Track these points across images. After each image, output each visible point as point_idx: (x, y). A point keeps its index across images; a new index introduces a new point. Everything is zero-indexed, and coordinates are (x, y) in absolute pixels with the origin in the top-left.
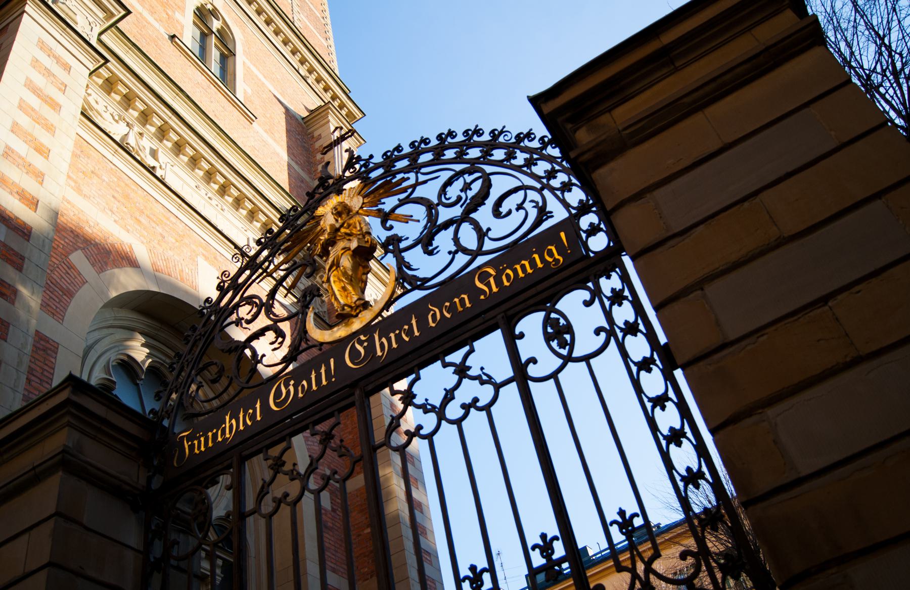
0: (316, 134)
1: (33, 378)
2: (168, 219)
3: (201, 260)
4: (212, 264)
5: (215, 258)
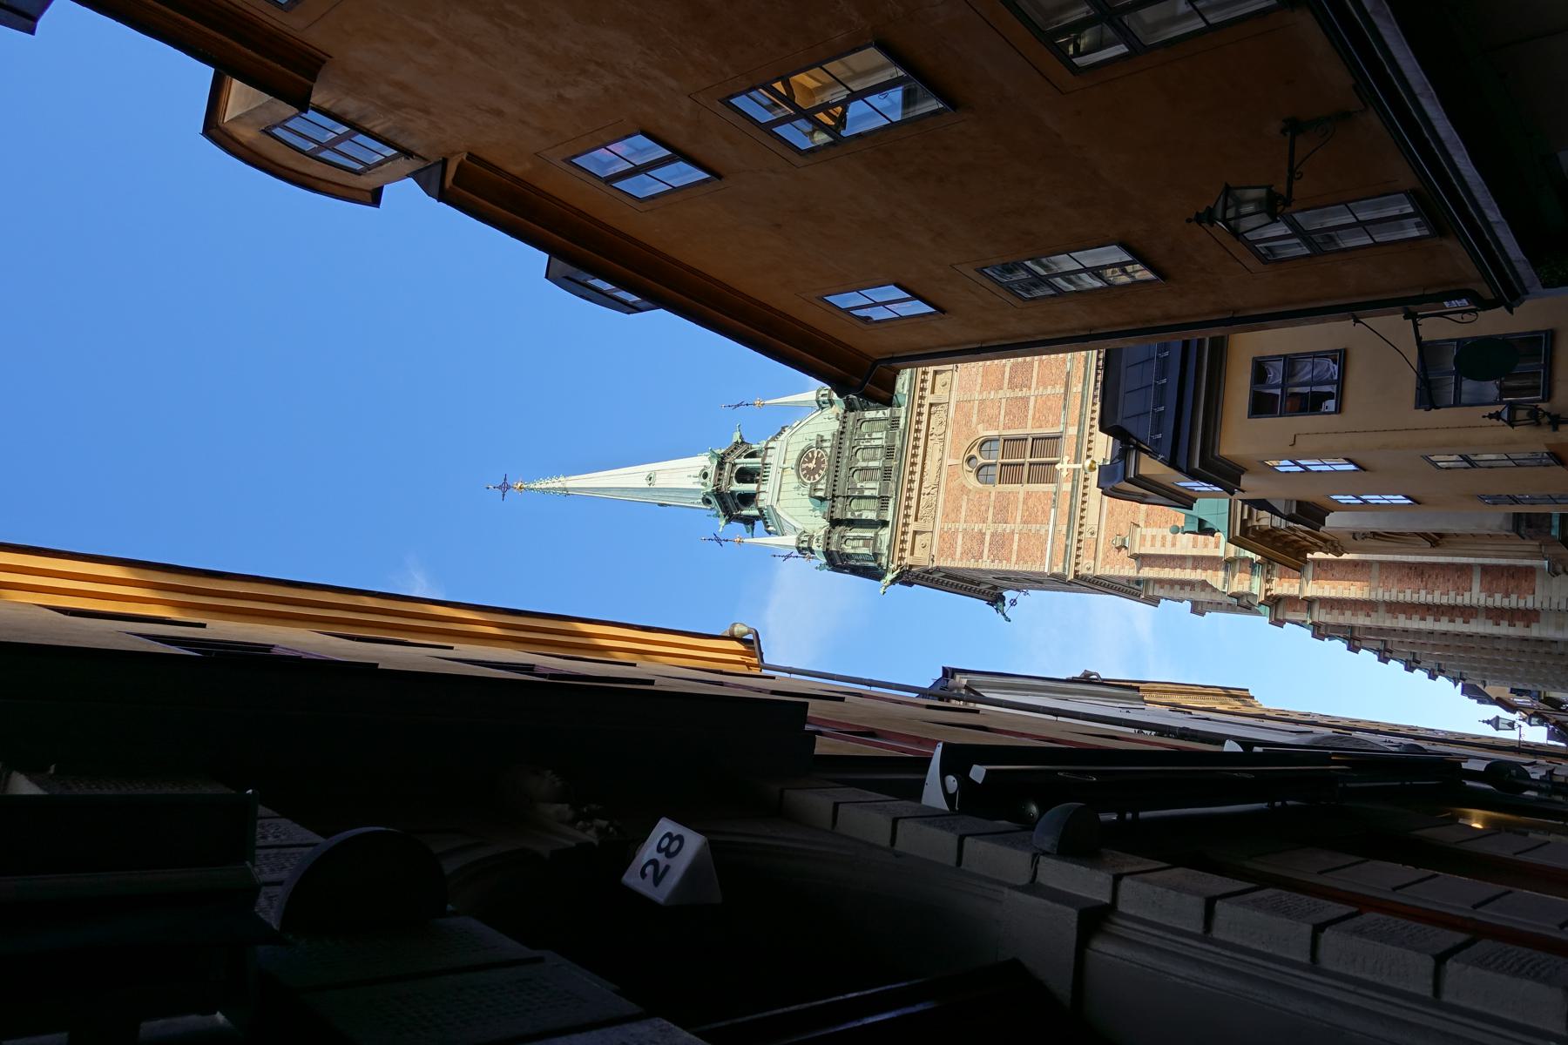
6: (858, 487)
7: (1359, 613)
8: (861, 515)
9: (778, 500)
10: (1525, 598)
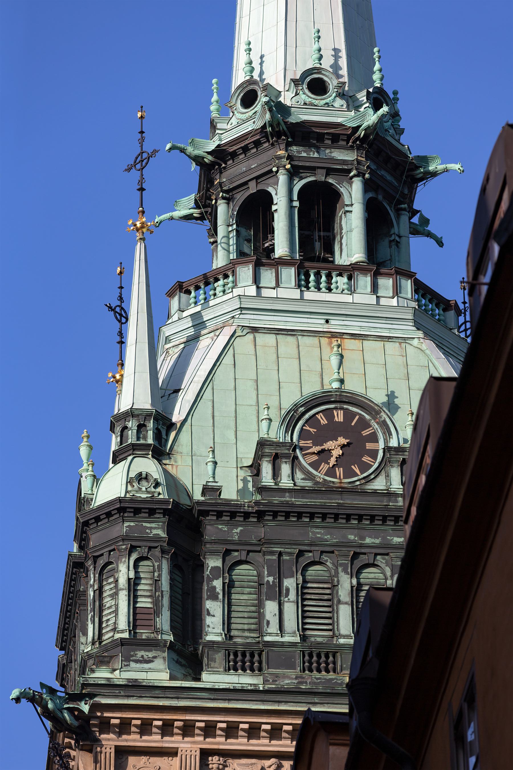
8: (214, 597)
9: (254, 330)
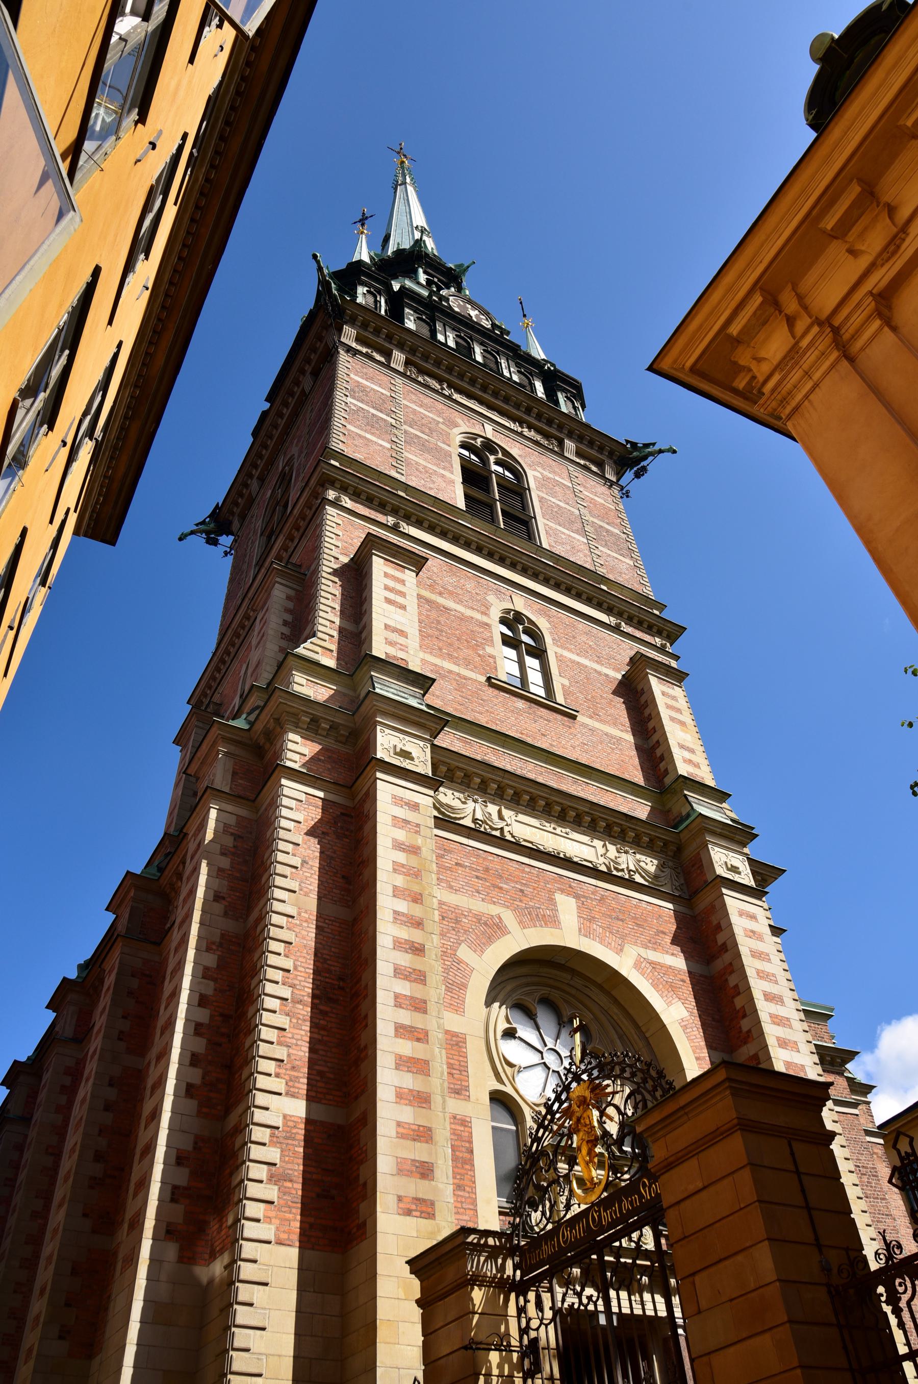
0: (639, 688)
1: (454, 1071)
2: (523, 871)
3: (559, 897)
4: (568, 895)
5: (570, 887)
6: (447, 333)
7: (225, 883)
10: (268, 1220)
